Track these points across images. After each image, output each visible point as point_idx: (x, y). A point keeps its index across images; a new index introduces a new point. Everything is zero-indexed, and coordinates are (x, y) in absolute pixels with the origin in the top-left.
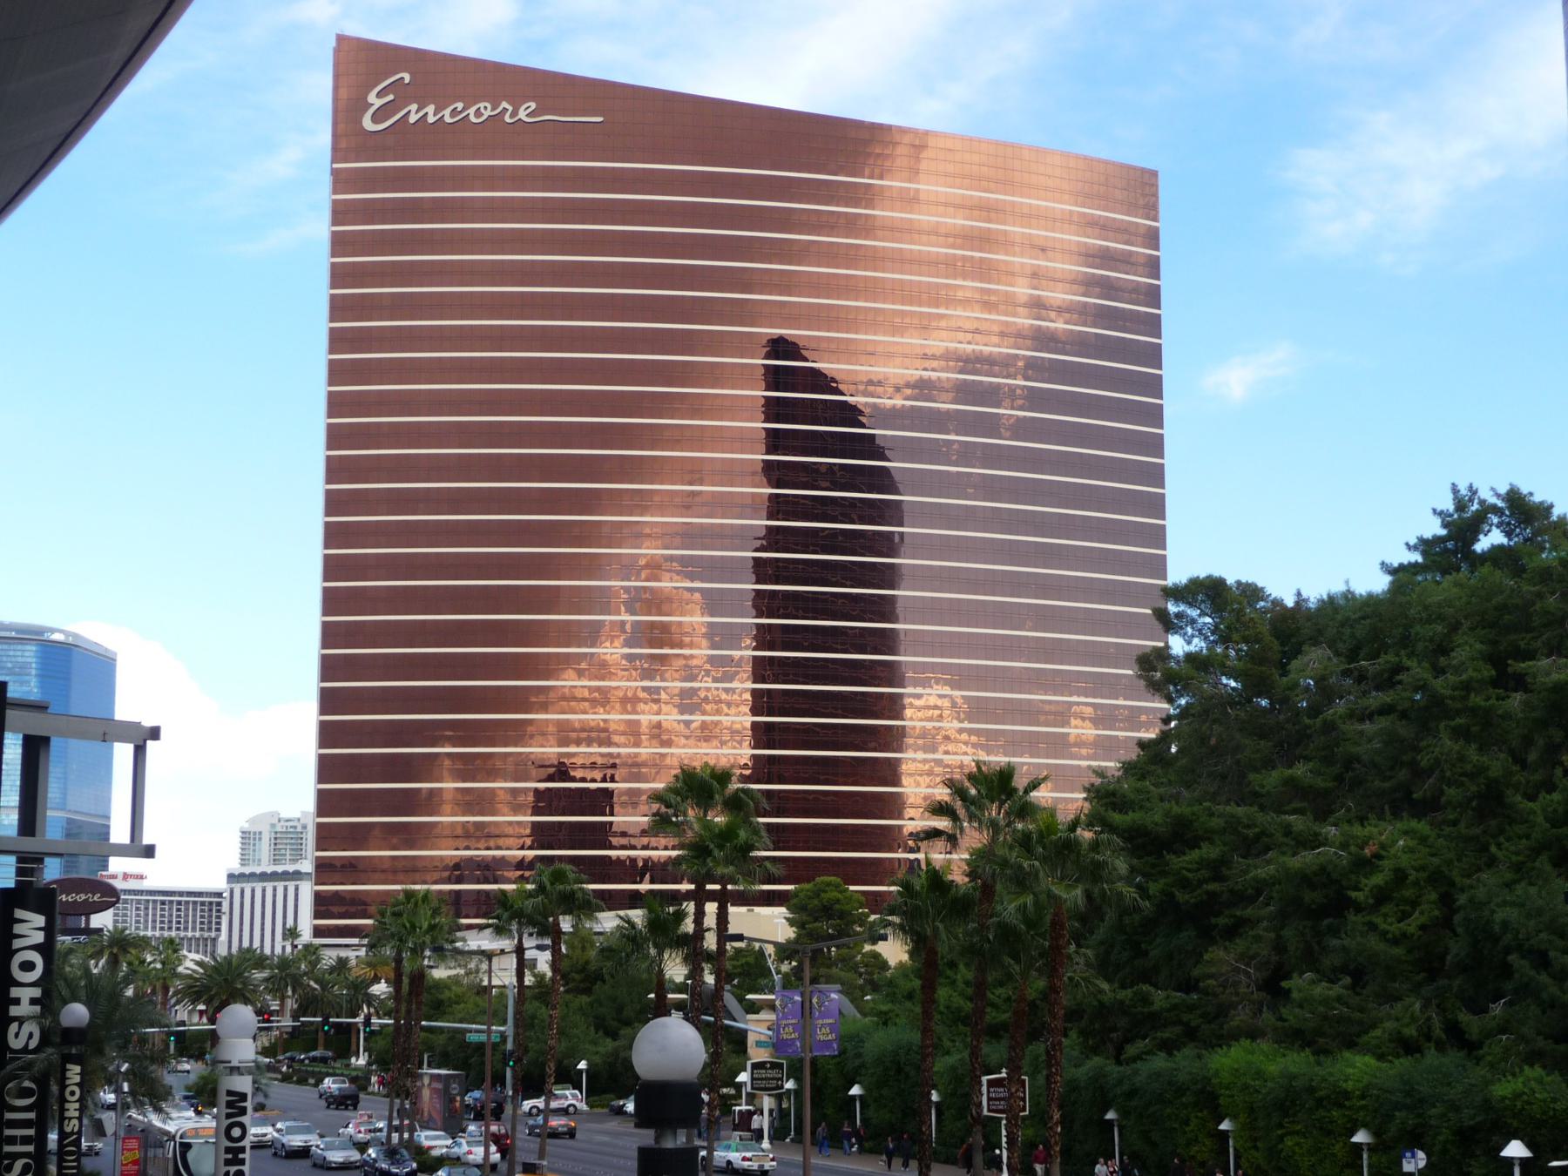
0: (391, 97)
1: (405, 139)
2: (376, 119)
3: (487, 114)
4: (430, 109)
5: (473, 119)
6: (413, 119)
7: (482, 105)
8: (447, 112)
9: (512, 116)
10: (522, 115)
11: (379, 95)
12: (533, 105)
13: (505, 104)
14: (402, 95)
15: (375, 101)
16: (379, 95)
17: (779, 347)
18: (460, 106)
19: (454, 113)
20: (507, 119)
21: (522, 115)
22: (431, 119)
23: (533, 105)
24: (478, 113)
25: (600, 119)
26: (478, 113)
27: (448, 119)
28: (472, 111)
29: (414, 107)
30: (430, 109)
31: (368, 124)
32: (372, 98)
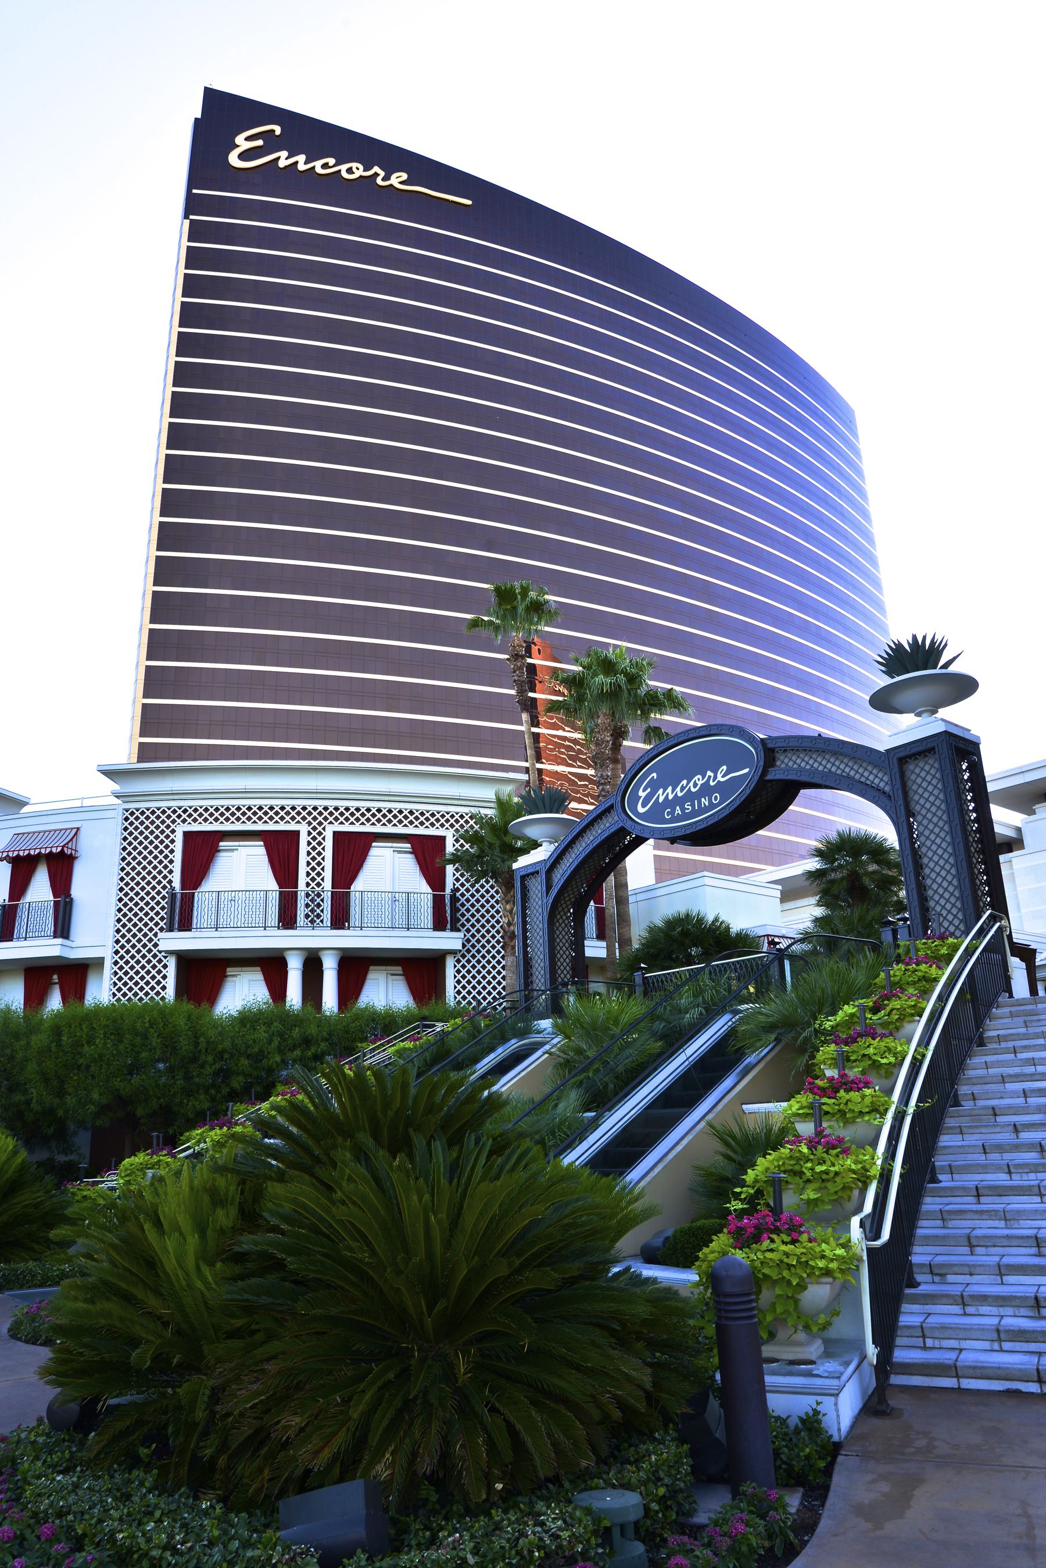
0: (260, 143)
3: (357, 174)
4: (301, 158)
6: (282, 163)
7: (354, 165)
8: (318, 165)
9: (383, 179)
11: (247, 139)
12: (404, 176)
13: (376, 169)
14: (272, 143)
15: (242, 142)
16: (247, 139)
18: (331, 161)
19: (325, 166)
22: (302, 167)
23: (404, 176)
24: (350, 171)
25: (469, 202)
26: (350, 171)
27: (319, 170)
28: (343, 168)
29: (284, 154)
30: (301, 158)
31: (233, 159)
32: (240, 139)
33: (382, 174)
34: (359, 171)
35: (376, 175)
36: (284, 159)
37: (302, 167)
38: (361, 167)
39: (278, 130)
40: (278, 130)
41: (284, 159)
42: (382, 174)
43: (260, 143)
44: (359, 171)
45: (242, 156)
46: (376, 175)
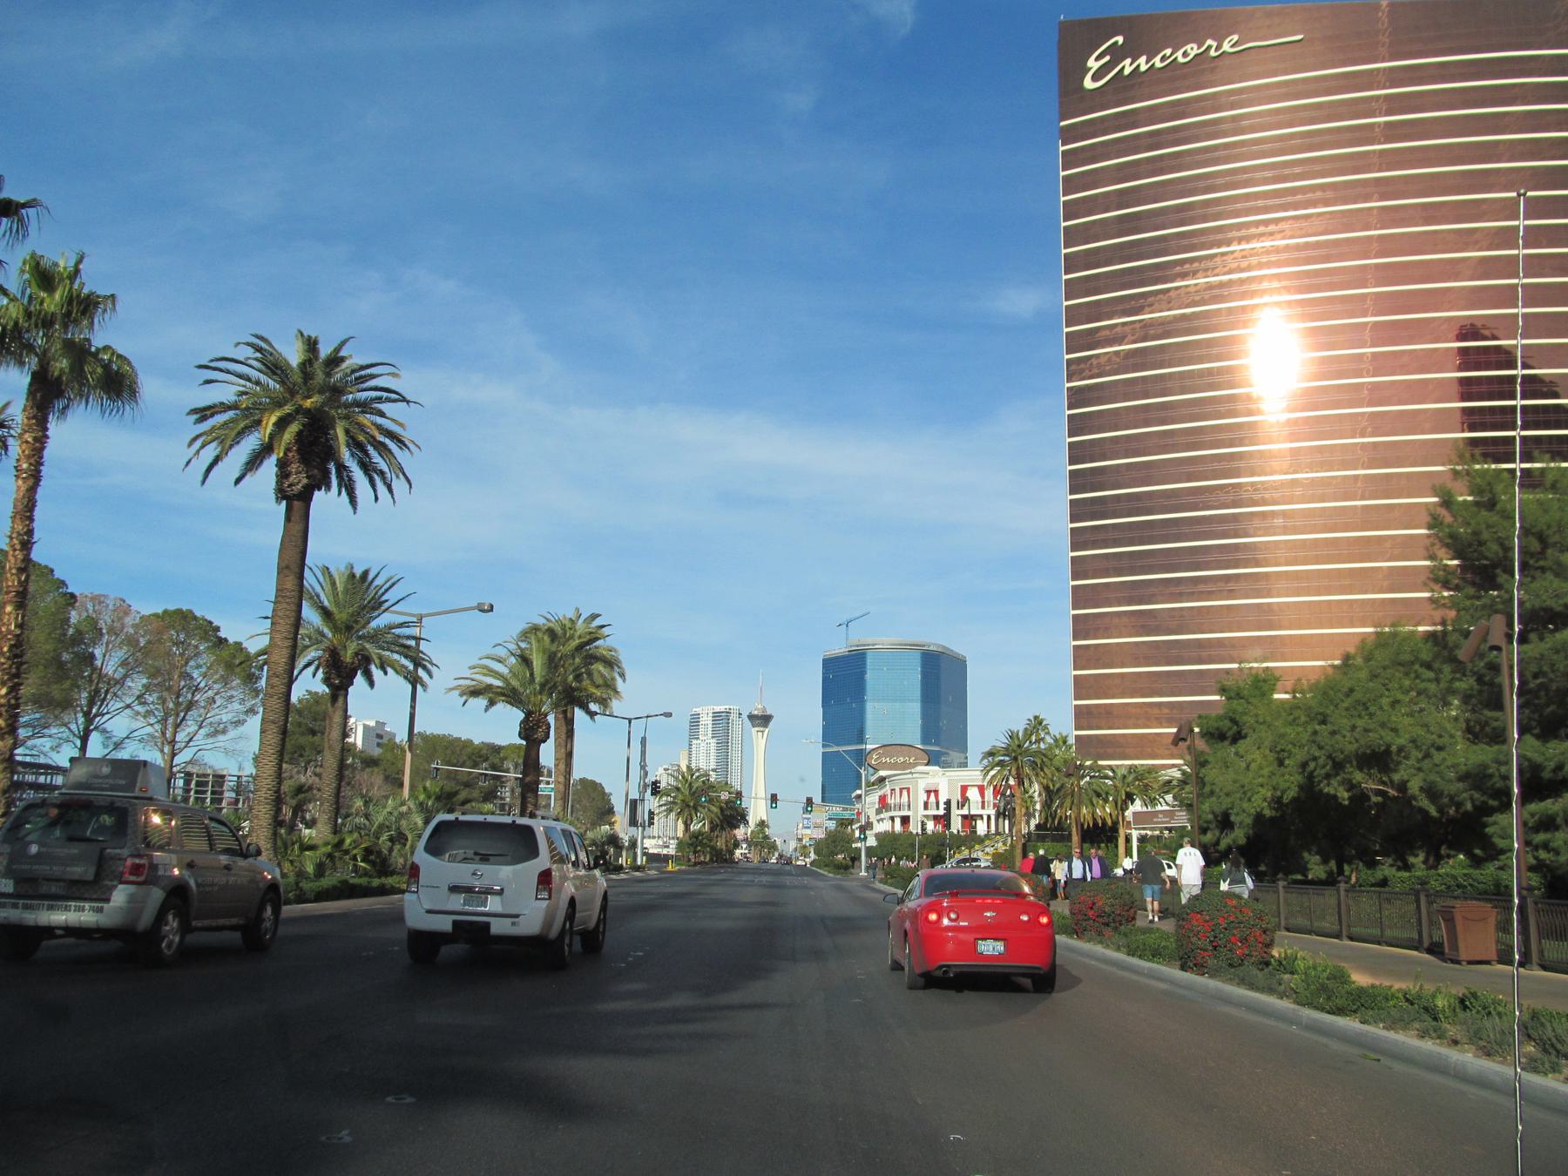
0: (1107, 58)
1: (1123, 88)
2: (1095, 78)
5: (1181, 60)
6: (1127, 72)
7: (1188, 47)
10: (1226, 47)
11: (1097, 59)
12: (1235, 38)
13: (1209, 42)
14: (1117, 54)
15: (1093, 64)
16: (1097, 59)
17: (1469, 331)
18: (1168, 52)
19: (1163, 59)
20: (1213, 53)
21: (1226, 47)
22: (1143, 68)
23: (1235, 38)
26: (1185, 54)
27: (1159, 65)
28: (1179, 54)
29: (1128, 61)
30: (1143, 59)
31: (1088, 84)
33: (1215, 44)
34: (1193, 50)
35: (1209, 47)
36: (1127, 66)
37: (1143, 68)
38: (1195, 46)
39: (1120, 39)
40: (1120, 39)
41: (1127, 66)
42: (1215, 44)
43: (1107, 58)
44: (1193, 50)
45: (1095, 78)
46: (1209, 47)
